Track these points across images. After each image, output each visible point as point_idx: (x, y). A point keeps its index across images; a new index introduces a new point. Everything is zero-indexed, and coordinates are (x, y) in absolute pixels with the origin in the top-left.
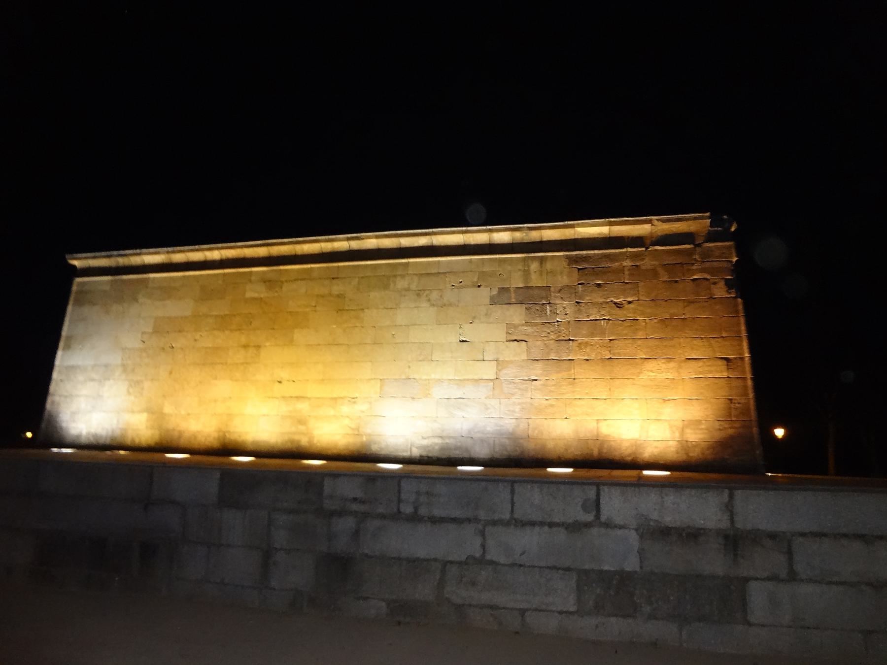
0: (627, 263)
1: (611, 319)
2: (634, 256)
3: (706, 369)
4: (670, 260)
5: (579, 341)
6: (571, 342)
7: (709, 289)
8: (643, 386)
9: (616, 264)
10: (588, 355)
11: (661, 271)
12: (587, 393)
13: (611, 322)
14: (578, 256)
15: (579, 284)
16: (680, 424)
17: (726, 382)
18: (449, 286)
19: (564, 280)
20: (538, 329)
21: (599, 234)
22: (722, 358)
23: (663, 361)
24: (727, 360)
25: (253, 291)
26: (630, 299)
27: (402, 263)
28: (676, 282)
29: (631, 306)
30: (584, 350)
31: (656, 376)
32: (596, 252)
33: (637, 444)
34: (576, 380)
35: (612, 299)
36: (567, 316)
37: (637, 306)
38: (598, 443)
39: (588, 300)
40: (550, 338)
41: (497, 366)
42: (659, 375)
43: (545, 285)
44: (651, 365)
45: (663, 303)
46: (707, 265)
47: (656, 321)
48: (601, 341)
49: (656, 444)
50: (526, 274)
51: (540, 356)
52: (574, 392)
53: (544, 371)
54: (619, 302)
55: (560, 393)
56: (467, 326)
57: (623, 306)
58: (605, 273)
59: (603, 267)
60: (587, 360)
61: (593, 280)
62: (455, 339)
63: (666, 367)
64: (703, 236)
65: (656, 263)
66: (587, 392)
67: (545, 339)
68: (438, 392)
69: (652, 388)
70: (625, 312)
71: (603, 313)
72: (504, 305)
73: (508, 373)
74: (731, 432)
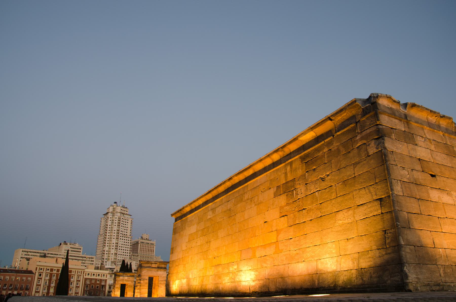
0: (326, 150)
1: (320, 190)
2: (329, 143)
3: (369, 210)
4: (344, 139)
5: (307, 209)
6: (304, 210)
7: (366, 150)
8: (336, 232)
9: (321, 153)
10: (311, 217)
11: (342, 149)
12: (311, 242)
13: (320, 191)
14: (305, 155)
15: (306, 172)
16: (357, 255)
17: (380, 218)
18: (260, 192)
19: (300, 172)
20: (291, 206)
21: (312, 137)
22: (377, 199)
23: (346, 210)
24: (381, 200)
25: (210, 215)
26: (328, 173)
27: (246, 185)
28: (349, 152)
29: (329, 177)
30: (310, 214)
31: (343, 223)
32: (311, 149)
33: (336, 274)
34: (307, 235)
35: (320, 176)
36: (302, 194)
37: (332, 176)
38: (318, 275)
39: (310, 181)
40: (296, 211)
41: (277, 233)
42: (344, 222)
43: (293, 178)
44: (340, 215)
45: (343, 170)
46: (364, 133)
47: (341, 183)
48: (316, 206)
49: (345, 273)
50: (286, 174)
51: (292, 223)
52: (306, 243)
53: (294, 232)
54: (323, 177)
55: (301, 245)
56: (266, 213)
57: (325, 179)
58: (316, 161)
59: (316, 157)
60: (311, 220)
61: (312, 167)
62: (262, 222)
63: (347, 215)
64: (360, 114)
65: (338, 144)
66: (311, 241)
67: (294, 212)
68: (259, 253)
69: (341, 232)
70: (326, 183)
71: (316, 187)
72: (278, 196)
73: (282, 236)
74: (386, 257)
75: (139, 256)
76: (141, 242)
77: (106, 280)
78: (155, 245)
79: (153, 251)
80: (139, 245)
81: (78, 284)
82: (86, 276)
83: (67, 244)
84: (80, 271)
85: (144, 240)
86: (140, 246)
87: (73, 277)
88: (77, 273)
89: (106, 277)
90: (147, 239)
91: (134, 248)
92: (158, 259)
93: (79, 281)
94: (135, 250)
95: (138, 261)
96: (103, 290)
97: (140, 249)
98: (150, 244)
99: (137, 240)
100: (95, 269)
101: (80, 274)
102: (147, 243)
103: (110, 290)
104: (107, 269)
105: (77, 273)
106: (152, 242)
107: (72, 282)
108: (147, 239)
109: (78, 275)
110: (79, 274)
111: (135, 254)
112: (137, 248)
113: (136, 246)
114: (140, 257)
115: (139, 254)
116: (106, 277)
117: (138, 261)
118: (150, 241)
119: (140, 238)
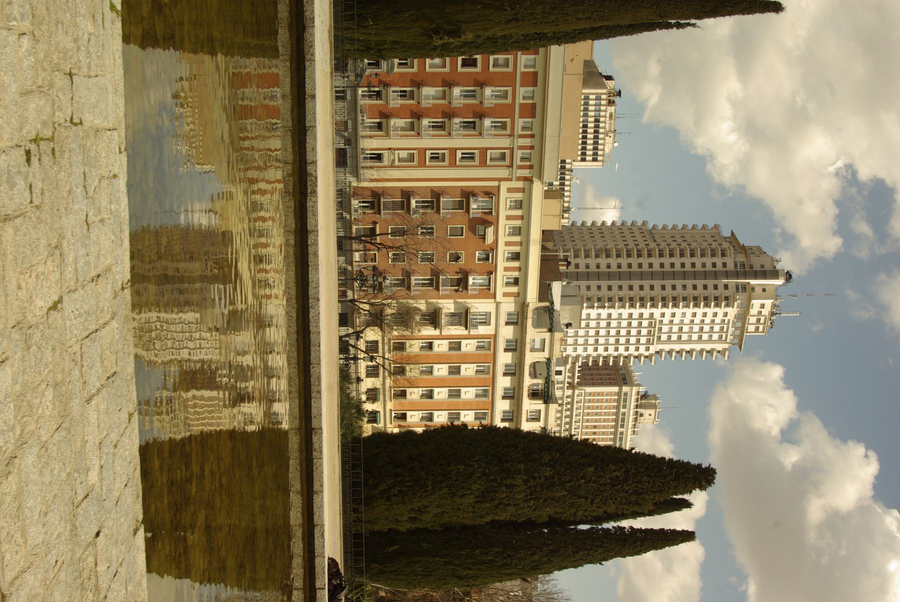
76: (626, 394)
77: (495, 298)
80: (615, 389)
81: (471, 157)
82: (510, 190)
84: (534, 161)
85: (637, 407)
87: (503, 126)
88: (521, 148)
89: (505, 295)
90: (642, 415)
93: (483, 164)
94: (592, 375)
96: (441, 288)
97: (599, 394)
99: (637, 375)
100: (543, 231)
101: (517, 162)
102: (623, 420)
103: (444, 320)
104: (545, 292)
105: (521, 148)
107: (474, 128)
108: (642, 415)
109: (512, 150)
110: (519, 154)
111: (577, 374)
112: (601, 379)
113: (609, 374)
115: (577, 392)
116: (505, 295)
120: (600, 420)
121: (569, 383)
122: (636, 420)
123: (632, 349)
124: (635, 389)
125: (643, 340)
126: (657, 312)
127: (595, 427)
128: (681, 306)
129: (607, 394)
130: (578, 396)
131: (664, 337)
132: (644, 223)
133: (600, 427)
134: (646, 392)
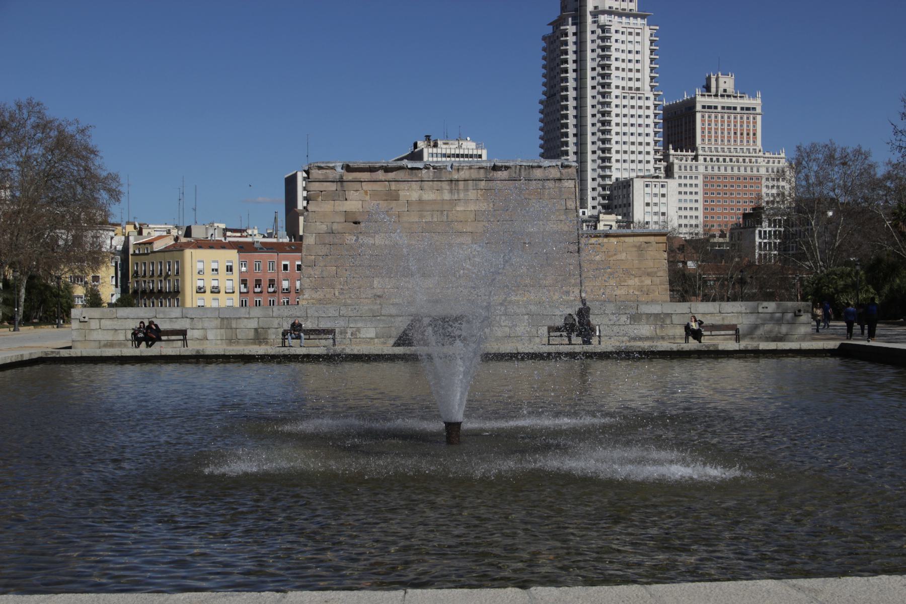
75: (701, 158)
76: (704, 107)
78: (759, 110)
79: (754, 134)
80: (698, 116)
83: (436, 145)
85: (716, 95)
86: (703, 121)
90: (725, 91)
91: (682, 133)
92: (776, 164)
95: (696, 178)
97: (703, 132)
98: (739, 110)
102: (729, 108)
106: (748, 102)
108: (725, 91)
112: (690, 130)
113: (686, 123)
114: (705, 160)
117: (696, 178)
118: (739, 101)
119: (697, 93)
120: (729, 130)
121: (692, 159)
122: (729, 96)
123: (647, 112)
124: (699, 98)
125: (640, 103)
126: (615, 92)
127: (735, 133)
128: (609, 72)
129: (703, 124)
130: (705, 151)
131: (638, 84)
132: (541, 102)
133: (735, 130)
134: (704, 87)
